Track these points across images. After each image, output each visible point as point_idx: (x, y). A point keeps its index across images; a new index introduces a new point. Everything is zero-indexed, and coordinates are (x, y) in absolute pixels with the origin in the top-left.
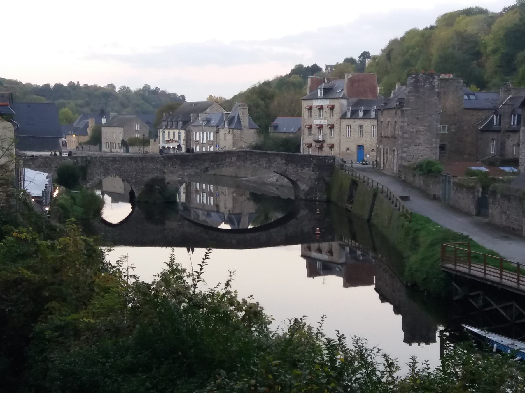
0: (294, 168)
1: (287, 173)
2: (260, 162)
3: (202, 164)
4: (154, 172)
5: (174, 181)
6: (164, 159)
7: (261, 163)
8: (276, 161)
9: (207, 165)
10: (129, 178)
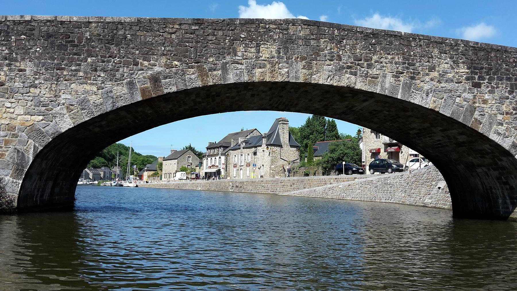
0: (502, 99)
1: (476, 115)
2: (370, 66)
3: (136, 64)
7: (374, 71)
8: (432, 69)
9: (157, 69)
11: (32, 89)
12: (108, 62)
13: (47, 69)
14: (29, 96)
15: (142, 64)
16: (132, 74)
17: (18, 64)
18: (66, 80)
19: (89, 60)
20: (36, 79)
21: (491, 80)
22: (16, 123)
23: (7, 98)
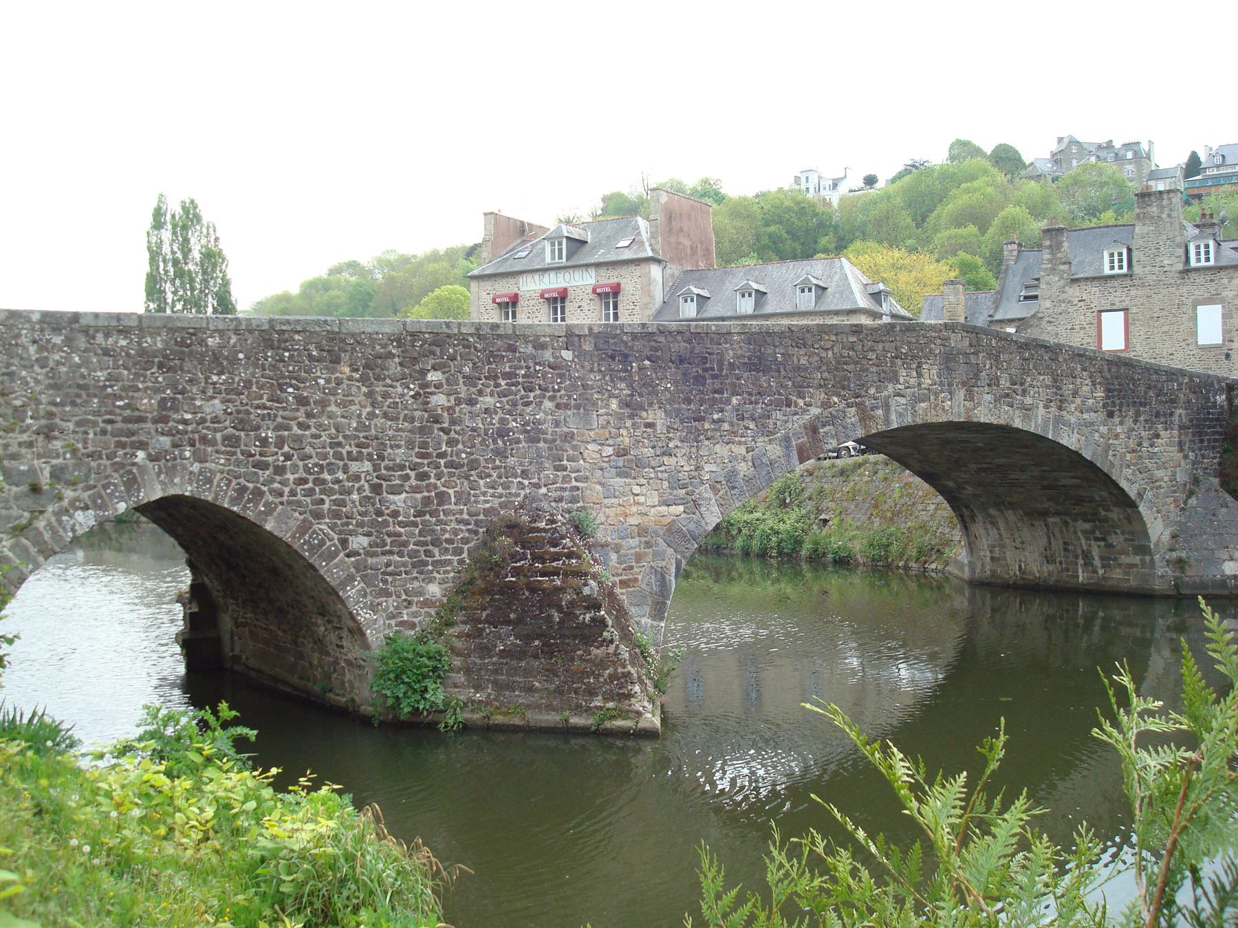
4: (511, 461)
5: (642, 531)
6: (580, 354)
7: (1028, 400)
9: (815, 411)
10: (318, 516)
11: (666, 459)
12: (756, 403)
13: (682, 421)
14: (662, 472)
15: (796, 405)
16: (786, 422)
17: (644, 414)
18: (707, 439)
19: (734, 400)
20: (670, 439)
21: (1121, 405)
22: (649, 521)
23: (634, 478)
